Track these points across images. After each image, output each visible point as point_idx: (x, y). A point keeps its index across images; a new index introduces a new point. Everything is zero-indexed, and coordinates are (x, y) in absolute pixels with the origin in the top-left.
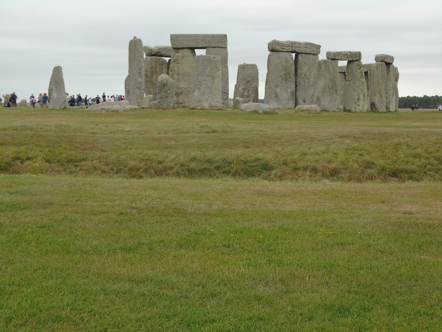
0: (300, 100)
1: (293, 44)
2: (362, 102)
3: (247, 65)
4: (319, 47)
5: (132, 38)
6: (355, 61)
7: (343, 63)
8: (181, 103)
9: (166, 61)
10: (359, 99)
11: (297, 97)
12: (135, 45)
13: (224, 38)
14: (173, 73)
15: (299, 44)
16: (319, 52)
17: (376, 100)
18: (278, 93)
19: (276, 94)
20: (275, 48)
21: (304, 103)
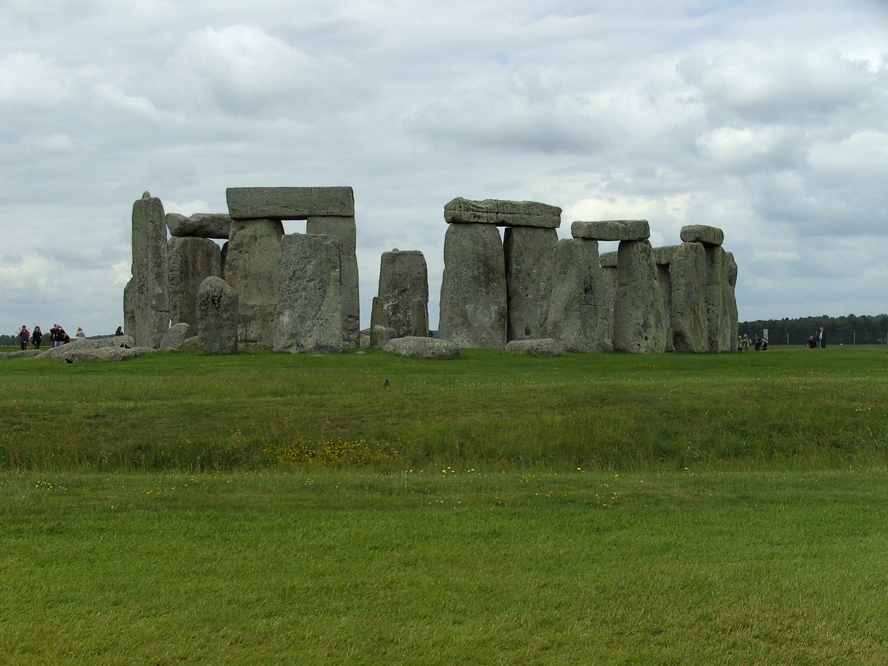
0: (519, 330)
3: (404, 254)
4: (557, 211)
6: (636, 241)
8: (252, 341)
9: (218, 247)
10: (646, 325)
11: (512, 322)
12: (147, 211)
13: (346, 195)
14: (235, 273)
16: (558, 223)
17: (685, 325)
19: (465, 317)
20: (461, 217)
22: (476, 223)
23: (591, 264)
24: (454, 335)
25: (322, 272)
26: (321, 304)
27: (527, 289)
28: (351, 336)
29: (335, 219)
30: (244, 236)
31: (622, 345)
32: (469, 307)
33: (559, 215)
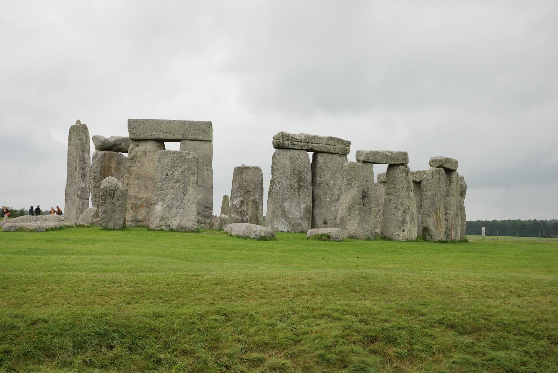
0: (319, 221)
1: (310, 139)
2: (409, 225)
3: (248, 168)
5: (74, 123)
6: (398, 165)
7: (380, 169)
8: (140, 221)
10: (404, 222)
11: (315, 215)
14: (130, 175)
15: (319, 138)
17: (431, 223)
18: (286, 209)
19: (283, 211)
20: (283, 144)
21: (325, 226)
22: (293, 149)
23: (368, 179)
24: (275, 223)
25: (185, 177)
26: (183, 198)
27: (326, 194)
28: (206, 221)
29: (198, 142)
30: (139, 151)
31: (387, 234)
32: (287, 205)
33: (349, 146)
